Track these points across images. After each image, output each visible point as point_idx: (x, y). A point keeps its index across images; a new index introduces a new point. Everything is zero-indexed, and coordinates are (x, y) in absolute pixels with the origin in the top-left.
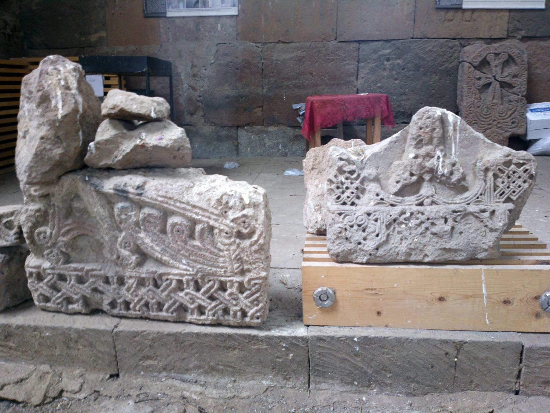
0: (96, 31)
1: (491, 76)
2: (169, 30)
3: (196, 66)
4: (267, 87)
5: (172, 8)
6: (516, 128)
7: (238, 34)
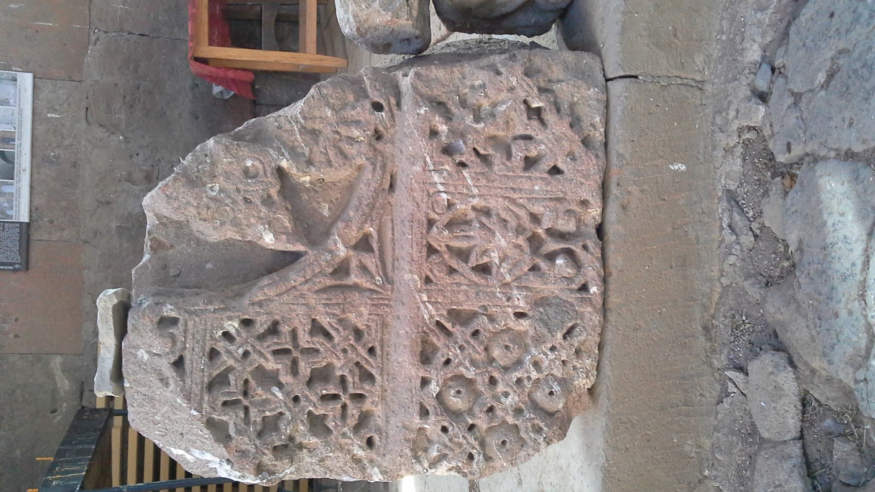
0: (51, 376)
2: (55, 222)
3: (130, 174)
4: (176, 30)
5: (12, 209)
7: (70, 77)
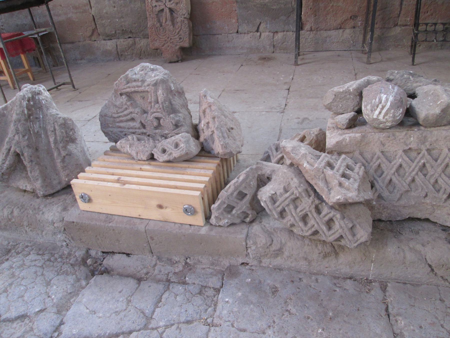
1: (163, 4)
6: (182, 43)
